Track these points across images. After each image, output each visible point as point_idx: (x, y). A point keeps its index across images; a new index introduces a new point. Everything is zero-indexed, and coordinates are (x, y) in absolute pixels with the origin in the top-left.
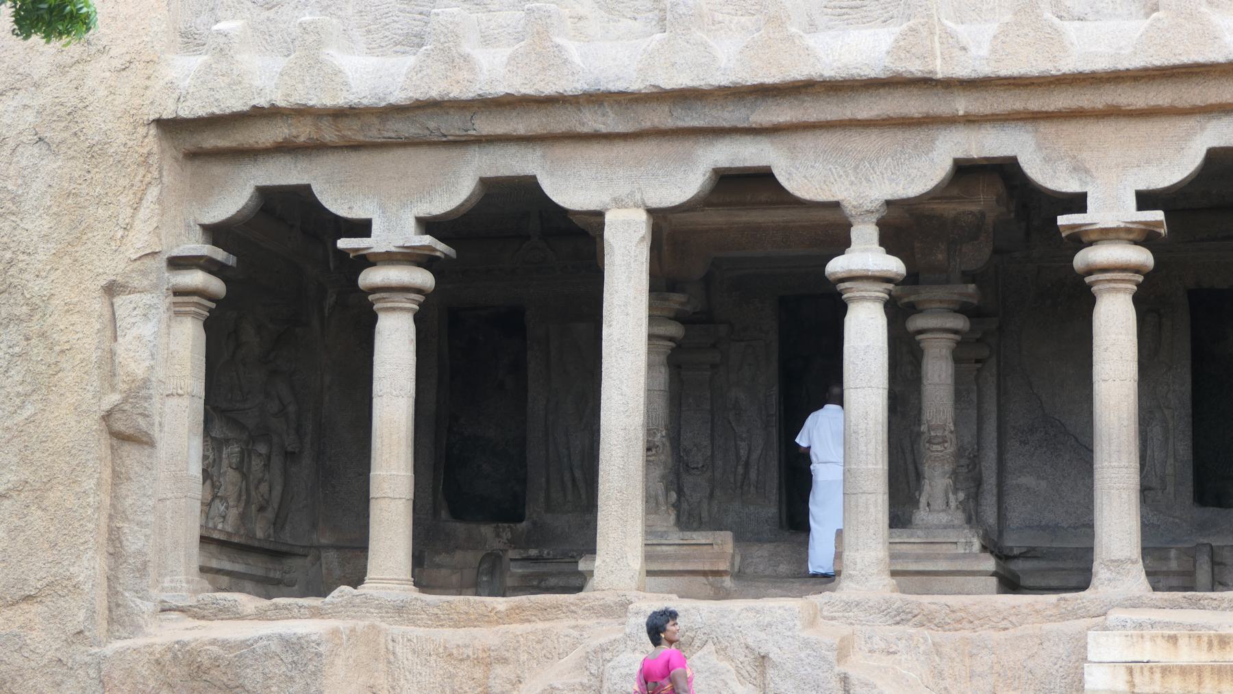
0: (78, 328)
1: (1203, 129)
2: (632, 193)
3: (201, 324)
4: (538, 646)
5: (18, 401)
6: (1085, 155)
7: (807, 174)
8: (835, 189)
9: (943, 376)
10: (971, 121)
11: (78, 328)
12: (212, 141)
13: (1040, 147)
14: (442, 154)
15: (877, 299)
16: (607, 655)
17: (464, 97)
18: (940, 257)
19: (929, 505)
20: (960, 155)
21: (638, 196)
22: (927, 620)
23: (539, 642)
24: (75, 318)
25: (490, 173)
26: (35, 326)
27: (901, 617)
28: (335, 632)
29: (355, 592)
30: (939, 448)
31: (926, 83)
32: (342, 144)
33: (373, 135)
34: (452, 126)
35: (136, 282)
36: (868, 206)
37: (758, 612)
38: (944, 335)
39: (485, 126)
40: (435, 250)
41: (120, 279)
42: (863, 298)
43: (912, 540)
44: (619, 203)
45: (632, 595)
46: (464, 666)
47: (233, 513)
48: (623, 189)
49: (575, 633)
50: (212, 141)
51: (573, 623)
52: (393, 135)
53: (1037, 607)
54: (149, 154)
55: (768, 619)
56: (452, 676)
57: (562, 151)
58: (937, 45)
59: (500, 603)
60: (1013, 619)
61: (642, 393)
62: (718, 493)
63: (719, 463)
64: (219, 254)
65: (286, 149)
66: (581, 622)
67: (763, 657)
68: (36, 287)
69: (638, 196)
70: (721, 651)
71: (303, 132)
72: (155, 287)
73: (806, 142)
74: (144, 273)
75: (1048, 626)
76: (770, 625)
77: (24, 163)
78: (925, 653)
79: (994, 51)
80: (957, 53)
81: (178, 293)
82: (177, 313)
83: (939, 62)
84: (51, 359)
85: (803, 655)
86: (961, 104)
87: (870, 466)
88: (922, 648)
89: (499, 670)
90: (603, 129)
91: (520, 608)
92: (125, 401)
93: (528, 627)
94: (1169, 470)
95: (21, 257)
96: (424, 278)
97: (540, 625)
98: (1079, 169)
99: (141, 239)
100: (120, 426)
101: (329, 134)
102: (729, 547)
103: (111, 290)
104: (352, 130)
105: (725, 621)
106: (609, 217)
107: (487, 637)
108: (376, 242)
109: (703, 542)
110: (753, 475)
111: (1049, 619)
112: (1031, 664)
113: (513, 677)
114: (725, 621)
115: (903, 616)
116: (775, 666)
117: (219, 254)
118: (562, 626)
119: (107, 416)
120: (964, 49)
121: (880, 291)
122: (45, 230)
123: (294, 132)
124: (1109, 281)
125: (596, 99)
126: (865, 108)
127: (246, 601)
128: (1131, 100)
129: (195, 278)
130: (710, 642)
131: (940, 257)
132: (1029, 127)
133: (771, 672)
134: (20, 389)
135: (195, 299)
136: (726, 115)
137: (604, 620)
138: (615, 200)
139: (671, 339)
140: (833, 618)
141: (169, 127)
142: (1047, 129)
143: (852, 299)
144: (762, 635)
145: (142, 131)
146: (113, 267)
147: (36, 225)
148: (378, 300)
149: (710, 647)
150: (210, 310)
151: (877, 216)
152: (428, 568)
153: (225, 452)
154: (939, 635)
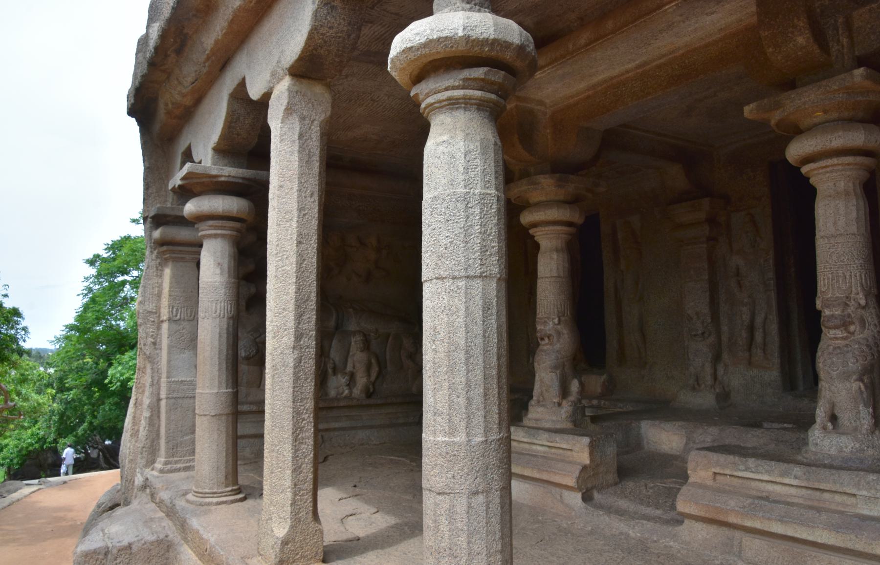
9: (841, 223)
18: (801, 40)
19: (833, 418)
30: (839, 333)
38: (835, 161)
43: (787, 481)
44: (276, 78)
47: (361, 381)
61: (291, 306)
62: (725, 356)
63: (725, 328)
87: (440, 439)
109: (565, 446)
110: (759, 337)
131: (801, 40)
139: (569, 224)
153: (353, 340)
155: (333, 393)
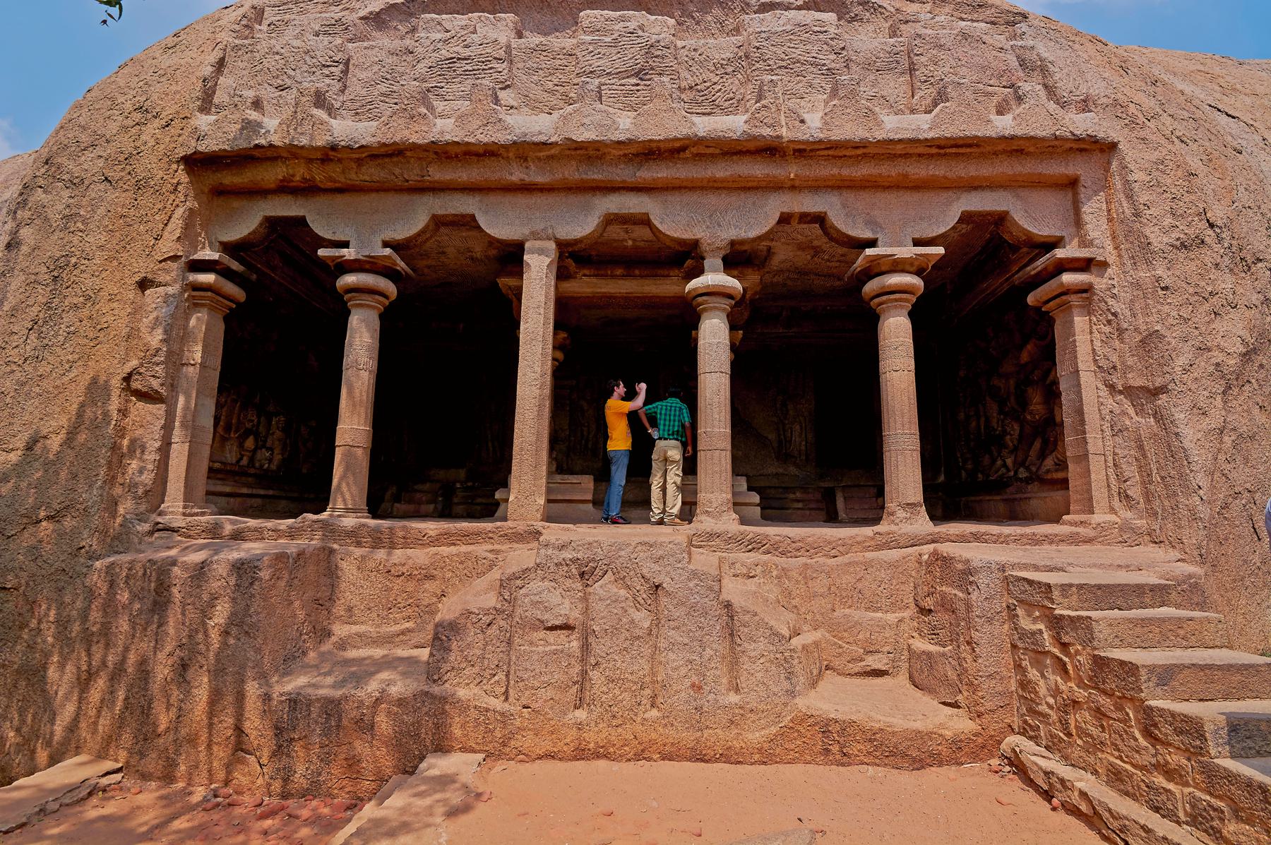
0: (116, 312)
1: (959, 198)
2: (545, 229)
3: (221, 317)
4: (461, 567)
5: (67, 366)
6: (876, 212)
7: (674, 221)
8: (695, 230)
10: (794, 187)
11: (116, 312)
12: (230, 179)
13: (844, 206)
14: (405, 197)
15: (724, 310)
16: (519, 582)
17: (420, 142)
20: (785, 210)
21: (550, 231)
22: (775, 548)
23: (461, 563)
24: (115, 305)
25: (440, 212)
26: (86, 312)
27: (754, 545)
28: (281, 557)
29: (315, 517)
31: (771, 150)
32: (329, 185)
33: (354, 177)
34: (412, 174)
35: (162, 278)
36: (718, 244)
37: (651, 546)
39: (438, 174)
40: (396, 265)
41: (150, 276)
42: (716, 308)
44: (535, 236)
45: (539, 525)
46: (399, 581)
47: (278, 457)
48: (539, 226)
49: (491, 556)
50: (230, 179)
51: (490, 547)
52: (367, 178)
53: (859, 539)
54: (178, 183)
55: (661, 552)
56: (388, 590)
57: (492, 199)
58: (782, 118)
59: (432, 527)
60: (841, 549)
64: (235, 266)
65: (286, 189)
66: (497, 547)
67: (657, 587)
68: (89, 282)
69: (550, 231)
70: (620, 580)
71: (300, 172)
72: (175, 281)
73: (674, 198)
74: (167, 271)
75: (869, 555)
76: (661, 557)
77: (93, 195)
78: (778, 577)
79: (826, 123)
80: (797, 123)
81: (197, 287)
82: (196, 305)
83: (784, 130)
84: (91, 335)
85: (691, 585)
86: (792, 171)
88: (775, 573)
89: (428, 585)
90: (527, 179)
91: (447, 534)
92: (142, 365)
93: (453, 549)
94: (803, 448)
95: (83, 262)
96: (390, 288)
97: (464, 549)
98: (871, 223)
99: (168, 245)
100: (136, 385)
101: (319, 175)
102: (591, 485)
103: (144, 285)
104: (336, 173)
105: (622, 553)
106: (527, 245)
107: (420, 556)
108: (348, 254)
111: (867, 549)
112: (859, 586)
113: (439, 592)
114: (622, 553)
115: (754, 545)
116: (668, 594)
117: (235, 266)
118: (481, 549)
119: (127, 379)
120: (802, 121)
121: (726, 304)
122: (102, 242)
123: (291, 171)
124: (896, 300)
125: (524, 151)
126: (721, 171)
127: (229, 523)
128: (917, 170)
129: (208, 278)
130: (610, 572)
132: (836, 193)
133: (664, 600)
134: (70, 357)
135: (209, 294)
136: (619, 171)
137: (515, 545)
138: (532, 233)
140: (700, 547)
141: (196, 163)
142: (850, 196)
143: (705, 310)
144: (656, 567)
145: (174, 166)
146: (142, 267)
147: (96, 238)
148: (350, 300)
149: (609, 576)
150: (230, 309)
151: (723, 253)
152: (378, 503)
154: (782, 561)
155: (257, 465)
